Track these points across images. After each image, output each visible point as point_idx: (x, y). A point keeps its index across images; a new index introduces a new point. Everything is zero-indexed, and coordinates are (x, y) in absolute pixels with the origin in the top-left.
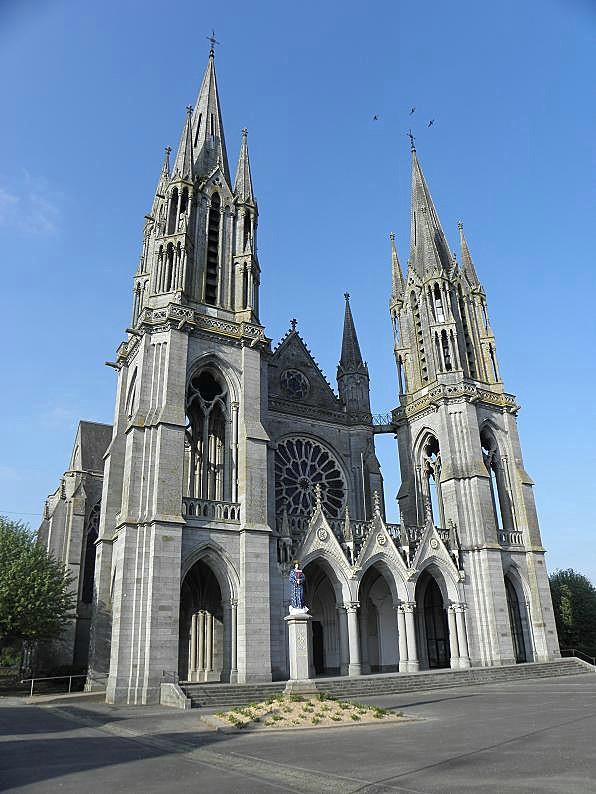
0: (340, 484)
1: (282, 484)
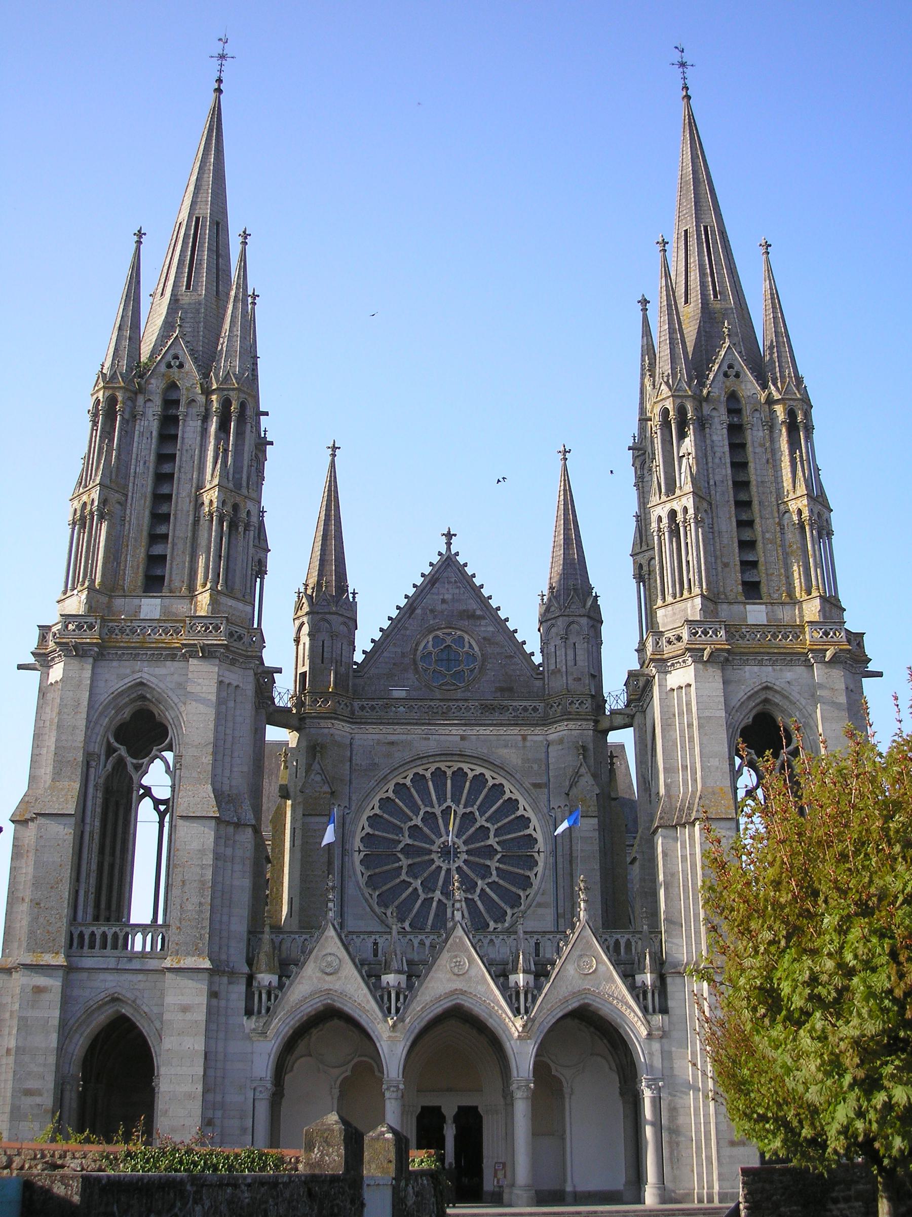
0: (531, 840)
1: (400, 855)
